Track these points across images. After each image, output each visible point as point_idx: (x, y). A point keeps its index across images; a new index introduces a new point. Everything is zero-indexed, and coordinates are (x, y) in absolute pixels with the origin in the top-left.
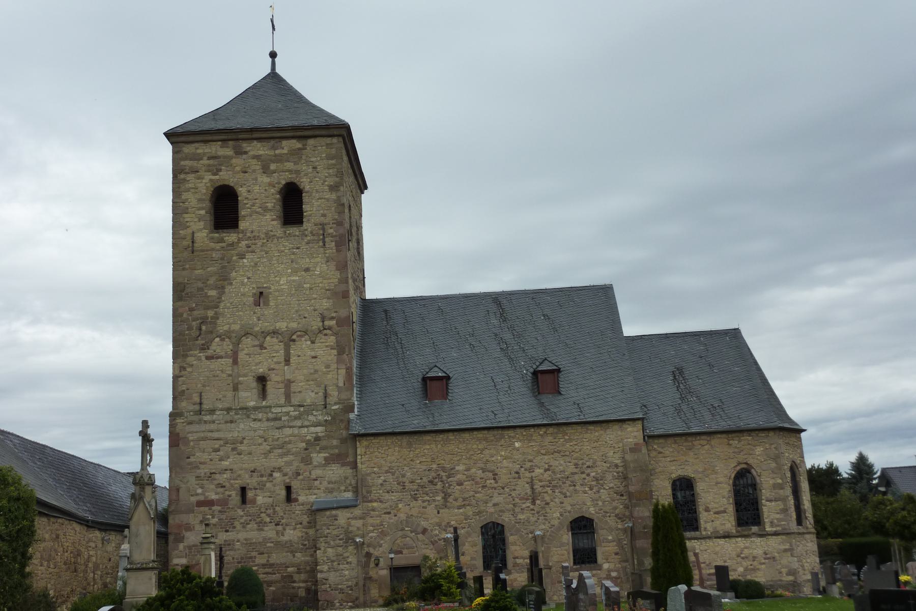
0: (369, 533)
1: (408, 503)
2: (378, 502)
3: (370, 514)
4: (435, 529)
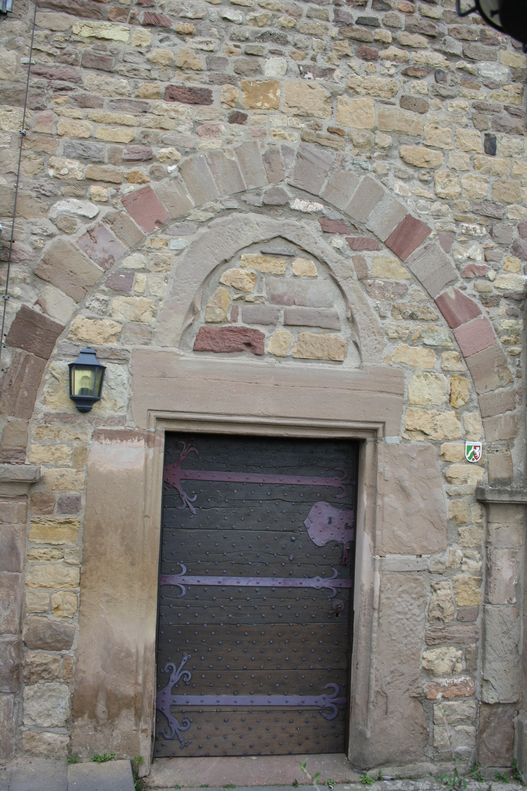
0: (54, 197)
1: (322, 63)
2: (133, 20)
3: (78, 81)
4: (469, 235)
